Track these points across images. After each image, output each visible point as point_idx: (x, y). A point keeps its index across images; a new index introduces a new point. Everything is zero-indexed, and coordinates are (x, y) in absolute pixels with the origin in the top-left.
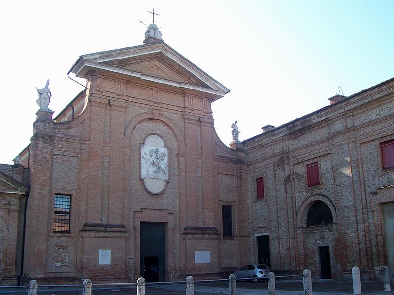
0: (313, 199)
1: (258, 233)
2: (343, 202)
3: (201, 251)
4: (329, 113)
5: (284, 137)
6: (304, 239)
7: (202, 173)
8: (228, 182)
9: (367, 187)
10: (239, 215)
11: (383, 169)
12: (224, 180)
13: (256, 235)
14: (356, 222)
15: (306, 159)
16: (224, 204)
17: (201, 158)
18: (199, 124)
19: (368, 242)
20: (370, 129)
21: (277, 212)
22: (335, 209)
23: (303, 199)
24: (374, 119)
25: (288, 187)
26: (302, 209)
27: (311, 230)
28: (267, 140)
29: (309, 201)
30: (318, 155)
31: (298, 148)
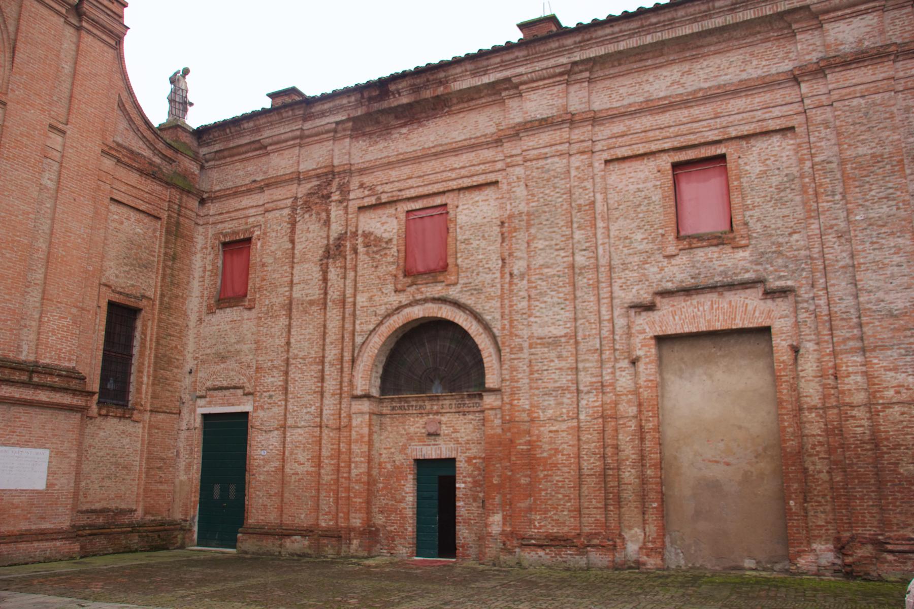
0: (417, 312)
2: (535, 327)
3: (13, 445)
4: (515, 63)
5: (340, 127)
6: (371, 434)
7: (59, 182)
8: (138, 234)
9: (616, 288)
10: (158, 343)
11: (678, 238)
12: (126, 223)
14: (574, 388)
16: (116, 298)
17: (63, 132)
18: (74, 21)
19: (609, 451)
20: (647, 121)
23: (382, 311)
24: (662, 95)
26: (377, 341)
27: (393, 408)
28: (284, 130)
29: (397, 321)
30: (454, 185)
31: (386, 161)
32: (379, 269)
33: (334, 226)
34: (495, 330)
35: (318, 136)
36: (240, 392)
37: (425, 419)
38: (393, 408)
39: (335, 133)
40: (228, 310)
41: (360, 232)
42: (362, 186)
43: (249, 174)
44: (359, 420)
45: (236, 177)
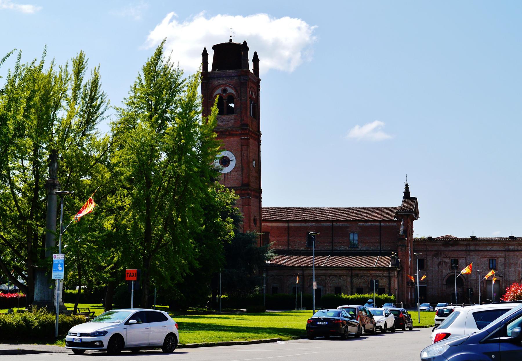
23: (447, 273)
25: (440, 267)
26: (447, 277)
33: (439, 260)
42: (444, 254)
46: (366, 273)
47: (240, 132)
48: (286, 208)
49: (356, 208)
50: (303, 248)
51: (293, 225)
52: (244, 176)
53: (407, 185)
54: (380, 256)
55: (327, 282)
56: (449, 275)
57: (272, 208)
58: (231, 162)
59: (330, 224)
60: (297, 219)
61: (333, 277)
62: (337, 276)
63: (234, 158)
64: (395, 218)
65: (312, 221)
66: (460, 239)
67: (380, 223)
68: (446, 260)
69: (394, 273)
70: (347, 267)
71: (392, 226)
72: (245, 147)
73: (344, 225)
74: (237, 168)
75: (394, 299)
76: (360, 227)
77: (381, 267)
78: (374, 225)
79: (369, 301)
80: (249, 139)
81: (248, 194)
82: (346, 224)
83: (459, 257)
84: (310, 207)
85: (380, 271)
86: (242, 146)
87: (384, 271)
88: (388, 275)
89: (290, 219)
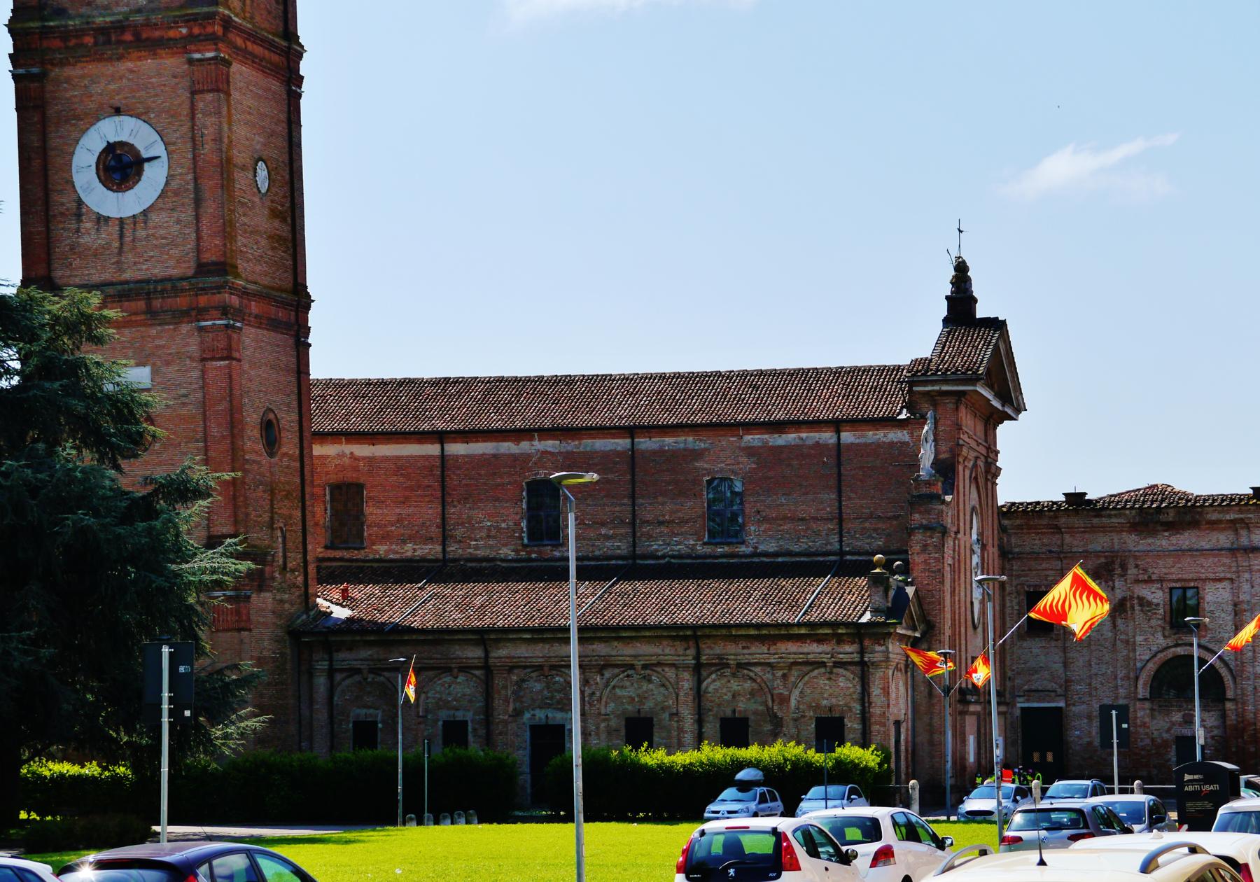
1: (1028, 701)
13: (1019, 705)
15: (1174, 577)
21: (1090, 665)
22: (1234, 678)
23: (1154, 649)
25: (1119, 621)
26: (1152, 667)
27: (1160, 706)
28: (1077, 522)
30: (1203, 576)
32: (1152, 621)
33: (1118, 591)
34: (1231, 666)
35: (1104, 529)
36: (1053, 694)
37: (1182, 713)
38: (1160, 706)
39: (1119, 530)
40: (1037, 639)
41: (1135, 596)
42: (1137, 566)
43: (1044, 545)
44: (1142, 713)
45: (1034, 545)
46: (758, 652)
47: (184, 31)
48: (447, 380)
49: (744, 374)
50: (507, 552)
51: (462, 452)
52: (205, 230)
53: (961, 269)
54: (833, 576)
55: (593, 693)
56: (1160, 655)
57: (383, 383)
58: (146, 165)
59: (622, 443)
60: (483, 425)
61: (617, 671)
62: (632, 667)
63: (159, 149)
64: (905, 410)
65: (544, 433)
66: (1205, 500)
67: (838, 432)
68: (1146, 592)
69: (883, 648)
70: (675, 627)
71: (891, 444)
72: (209, 97)
73: (682, 446)
74: (176, 193)
75: (880, 765)
76: (751, 451)
77: (825, 624)
78: (810, 442)
79: (741, 775)
80: (228, 64)
81: (225, 311)
82: (690, 439)
83: (1204, 580)
84: (547, 372)
85: (820, 640)
86: (193, 93)
87: (840, 640)
88: (856, 657)
89: (454, 426)
